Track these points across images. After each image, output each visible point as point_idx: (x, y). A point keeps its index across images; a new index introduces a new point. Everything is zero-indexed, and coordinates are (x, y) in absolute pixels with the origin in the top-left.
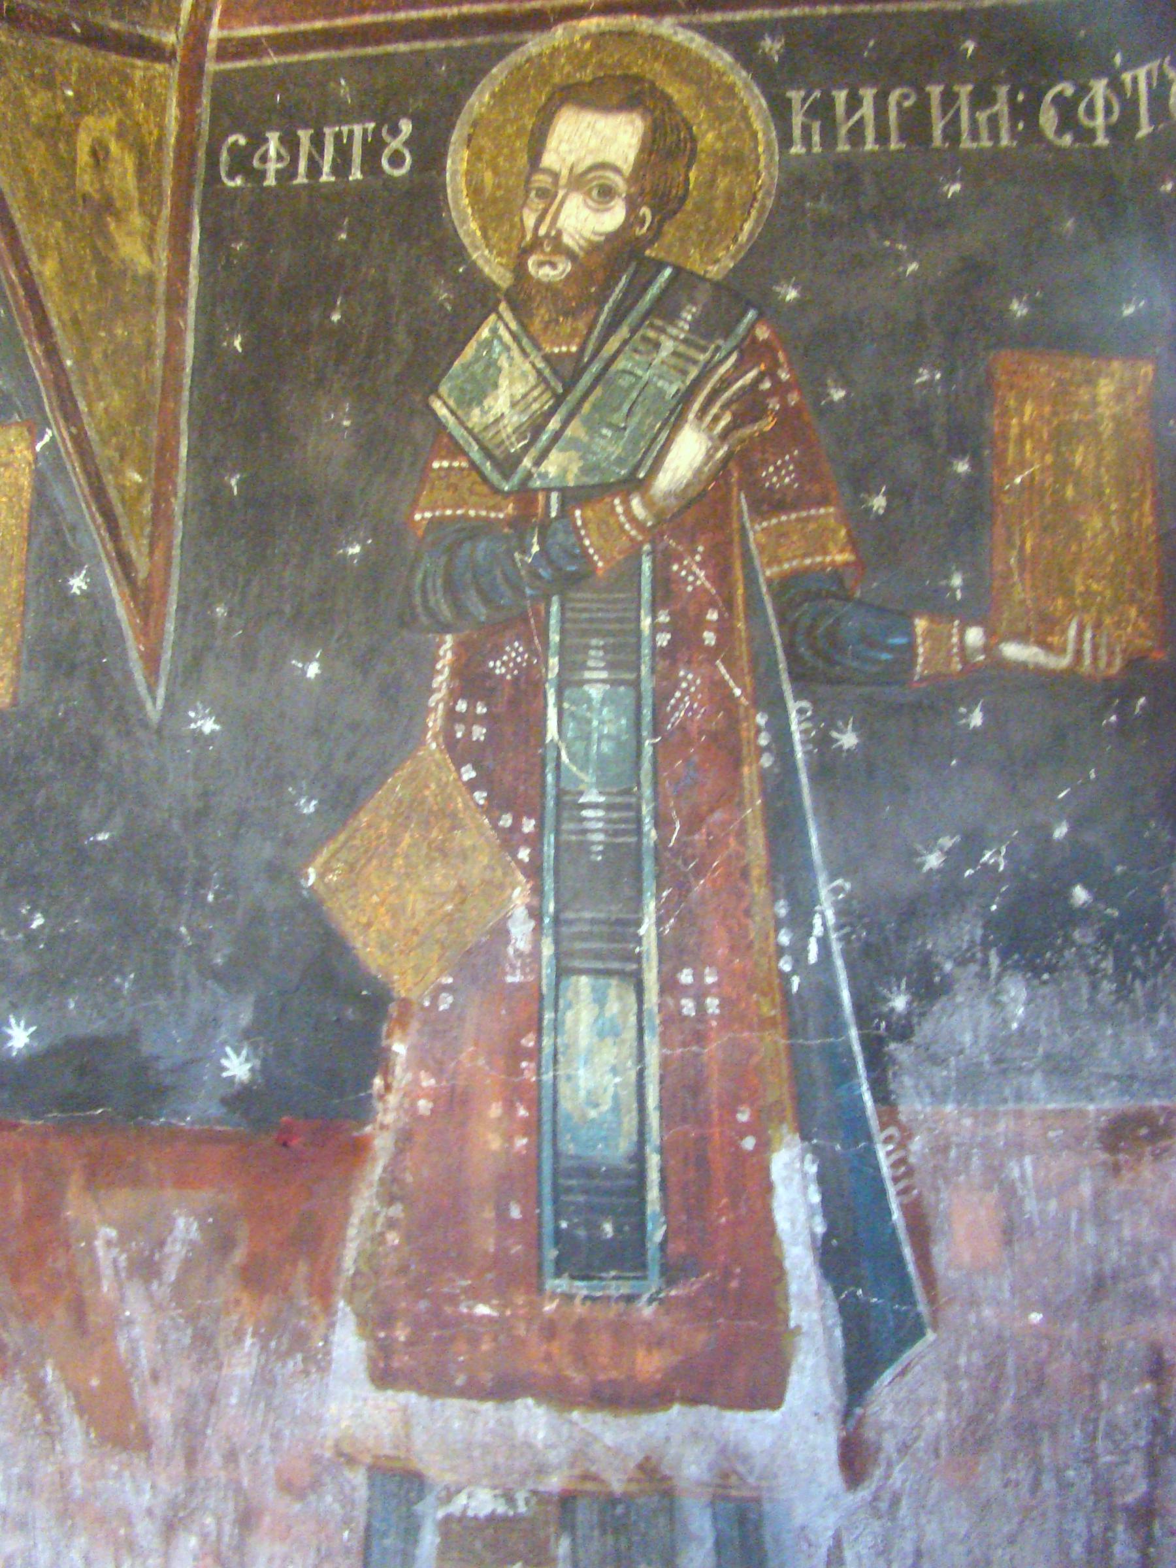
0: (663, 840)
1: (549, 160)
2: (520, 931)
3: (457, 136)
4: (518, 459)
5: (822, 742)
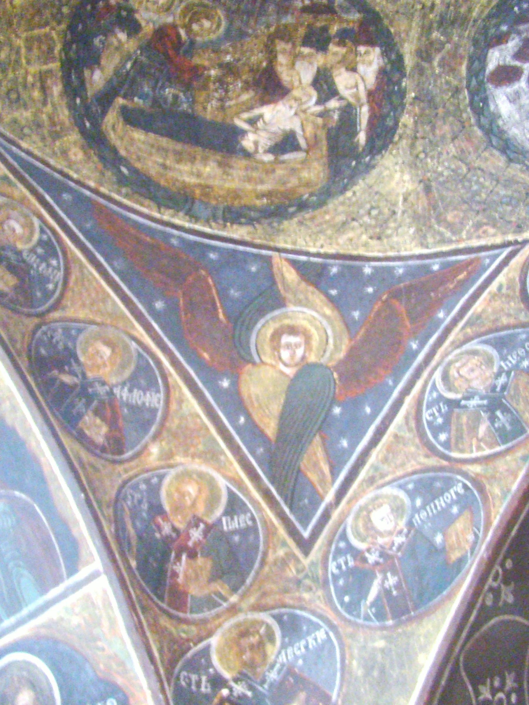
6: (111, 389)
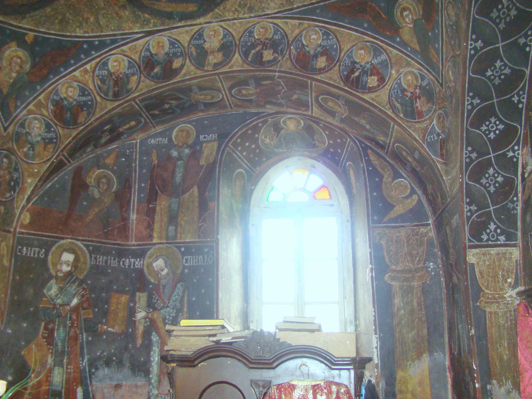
0: (68, 350)
1: (62, 259)
4: (54, 299)
5: (87, 339)
6: (371, 63)
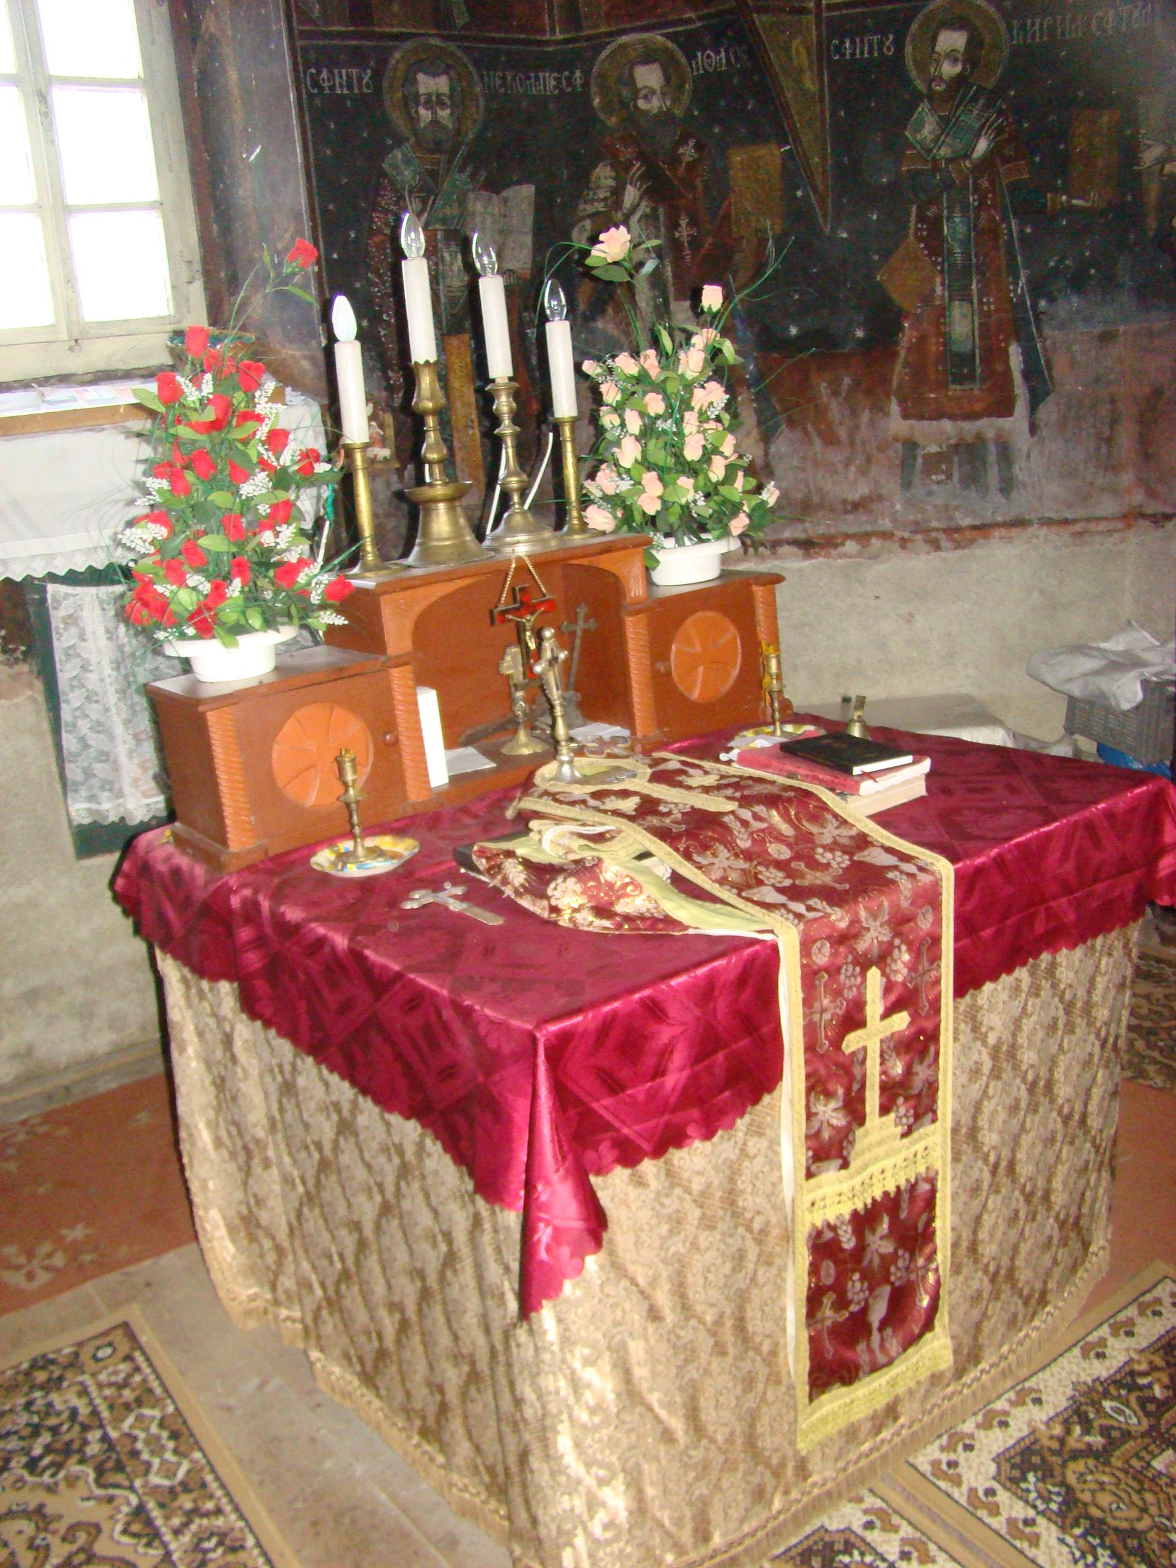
1: (937, 49)
2: (939, 290)
3: (908, 40)
5: (1021, 231)
